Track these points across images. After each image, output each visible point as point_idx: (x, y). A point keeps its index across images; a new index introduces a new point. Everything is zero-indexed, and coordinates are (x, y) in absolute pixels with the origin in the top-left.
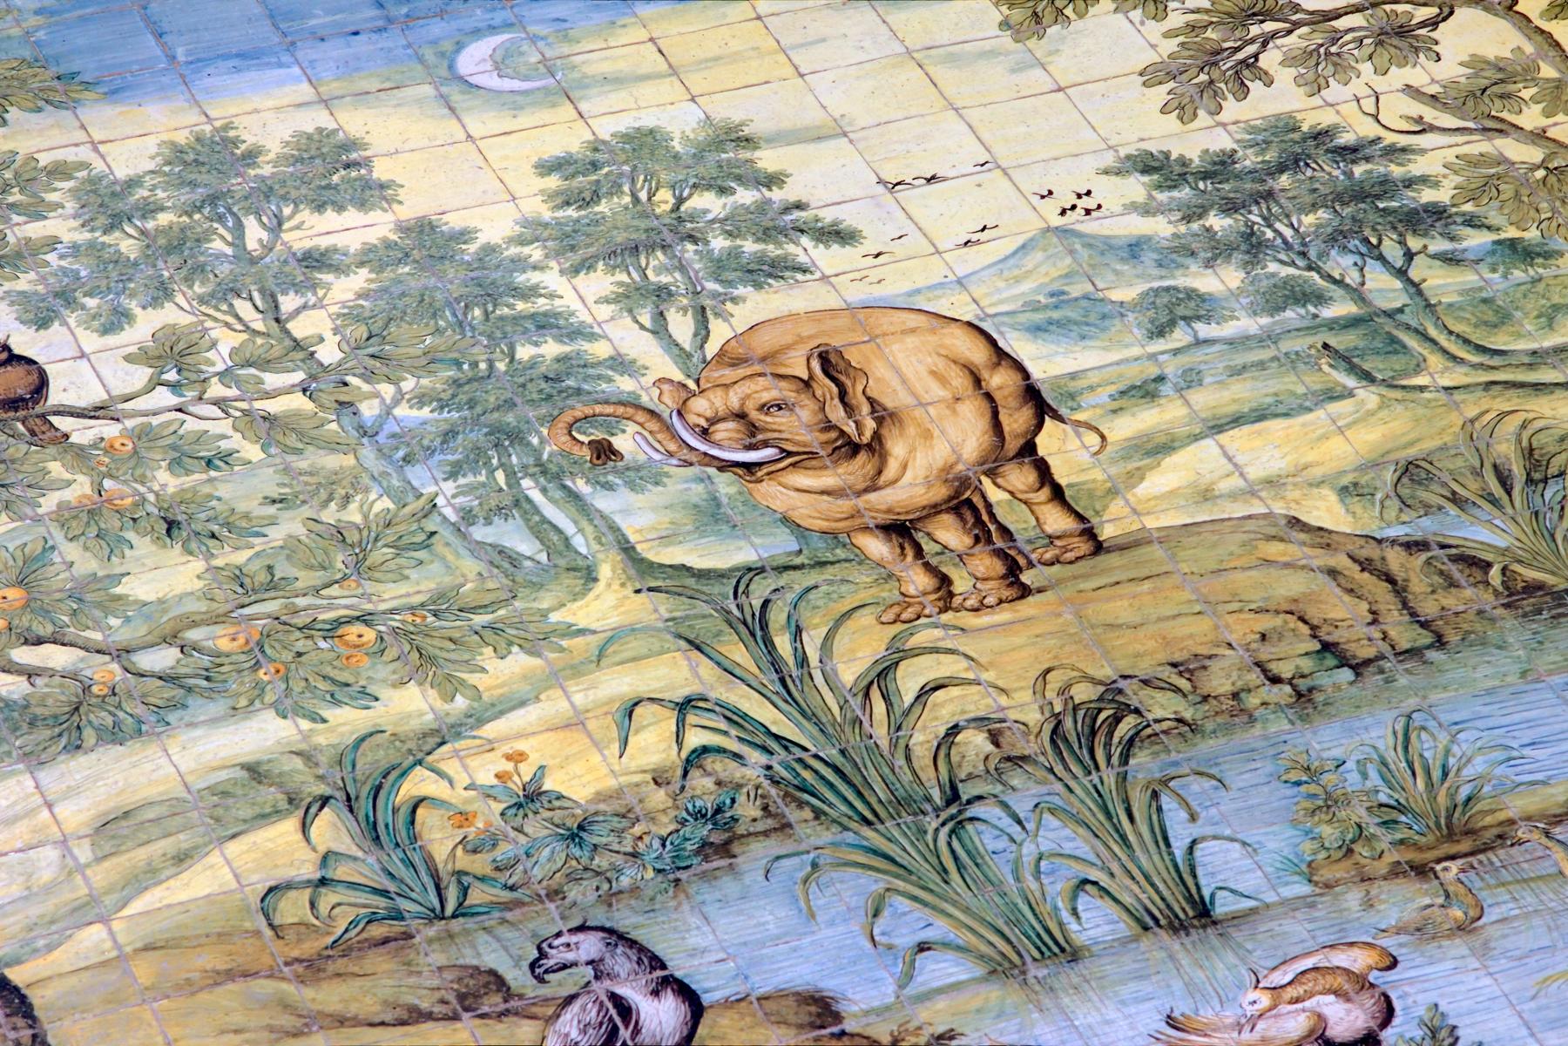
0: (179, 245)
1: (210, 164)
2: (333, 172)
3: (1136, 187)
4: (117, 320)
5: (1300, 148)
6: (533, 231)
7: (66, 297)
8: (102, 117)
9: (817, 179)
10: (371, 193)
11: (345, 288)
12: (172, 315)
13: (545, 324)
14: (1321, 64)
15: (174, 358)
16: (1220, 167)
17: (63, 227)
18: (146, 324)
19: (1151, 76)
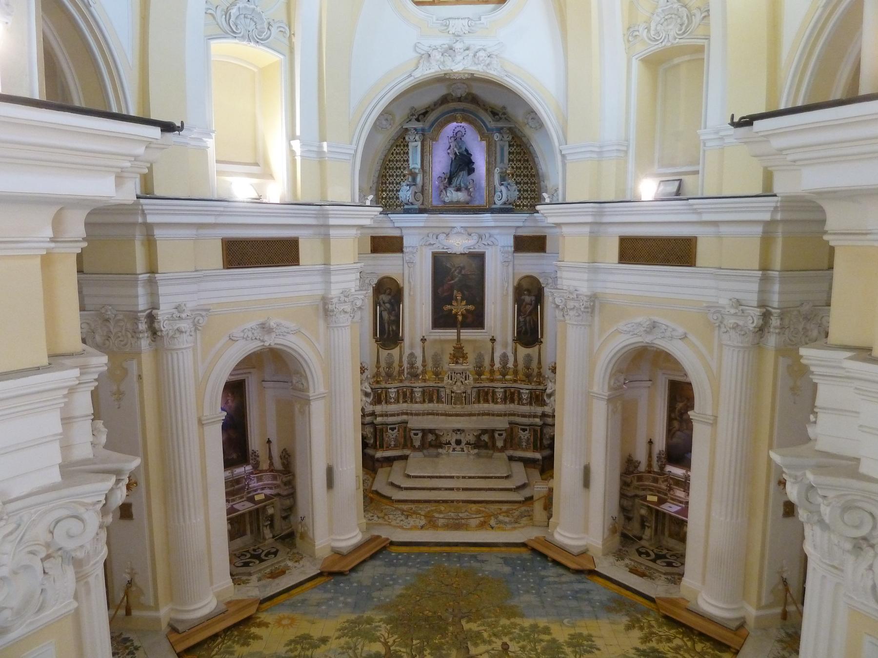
0: (528, 636)
1: (534, 628)
2: (546, 631)
3: (634, 651)
4: (518, 642)
5: (654, 650)
6: (566, 642)
7: (514, 639)
8: (525, 620)
9: (598, 643)
10: (550, 634)
11: (543, 644)
12: (525, 643)
13: (563, 653)
14: (659, 641)
15: (523, 648)
16: (644, 651)
17: (517, 631)
18: (522, 643)
19: (641, 638)
